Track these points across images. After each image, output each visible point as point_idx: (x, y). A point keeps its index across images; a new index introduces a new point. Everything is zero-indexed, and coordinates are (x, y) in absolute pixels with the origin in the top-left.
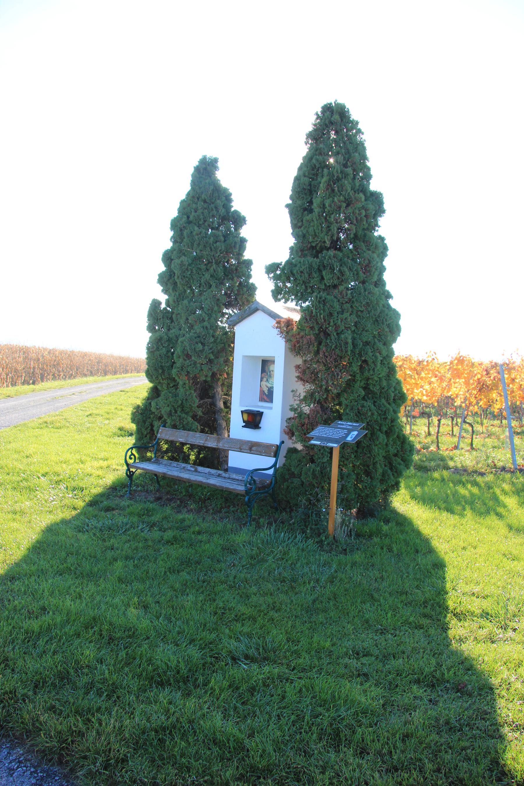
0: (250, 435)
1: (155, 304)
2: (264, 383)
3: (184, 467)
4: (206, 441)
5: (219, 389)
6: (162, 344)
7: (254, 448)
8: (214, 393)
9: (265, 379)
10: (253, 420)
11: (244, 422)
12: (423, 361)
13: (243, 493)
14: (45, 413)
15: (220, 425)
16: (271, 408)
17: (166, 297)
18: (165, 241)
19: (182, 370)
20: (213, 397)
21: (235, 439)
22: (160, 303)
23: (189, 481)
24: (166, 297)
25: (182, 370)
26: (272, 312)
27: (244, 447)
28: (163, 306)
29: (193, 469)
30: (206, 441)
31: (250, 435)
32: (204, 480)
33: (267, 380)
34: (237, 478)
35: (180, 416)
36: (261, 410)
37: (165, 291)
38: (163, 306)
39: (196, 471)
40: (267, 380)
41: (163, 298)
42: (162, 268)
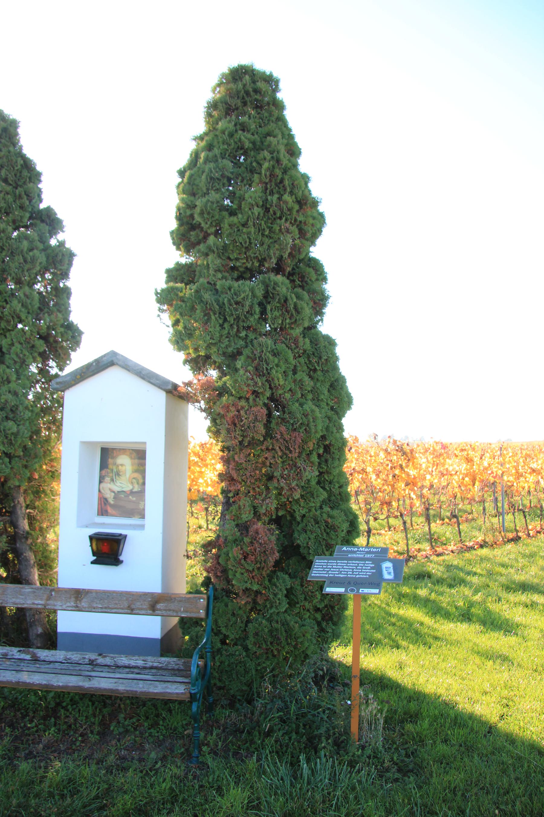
0: (104, 578)
2: (107, 485)
4: (49, 598)
5: (21, 499)
7: (159, 606)
8: (15, 506)
9: (108, 479)
10: (108, 549)
14: (127, 731)
15: (27, 560)
16: (142, 527)
18: (52, 195)
20: (12, 513)
21: (114, 592)
23: (47, 689)
26: (143, 369)
29: (28, 657)
30: (49, 598)
31: (104, 578)
32: (87, 684)
34: (133, 663)
36: (123, 532)
39: (36, 659)
40: (112, 480)
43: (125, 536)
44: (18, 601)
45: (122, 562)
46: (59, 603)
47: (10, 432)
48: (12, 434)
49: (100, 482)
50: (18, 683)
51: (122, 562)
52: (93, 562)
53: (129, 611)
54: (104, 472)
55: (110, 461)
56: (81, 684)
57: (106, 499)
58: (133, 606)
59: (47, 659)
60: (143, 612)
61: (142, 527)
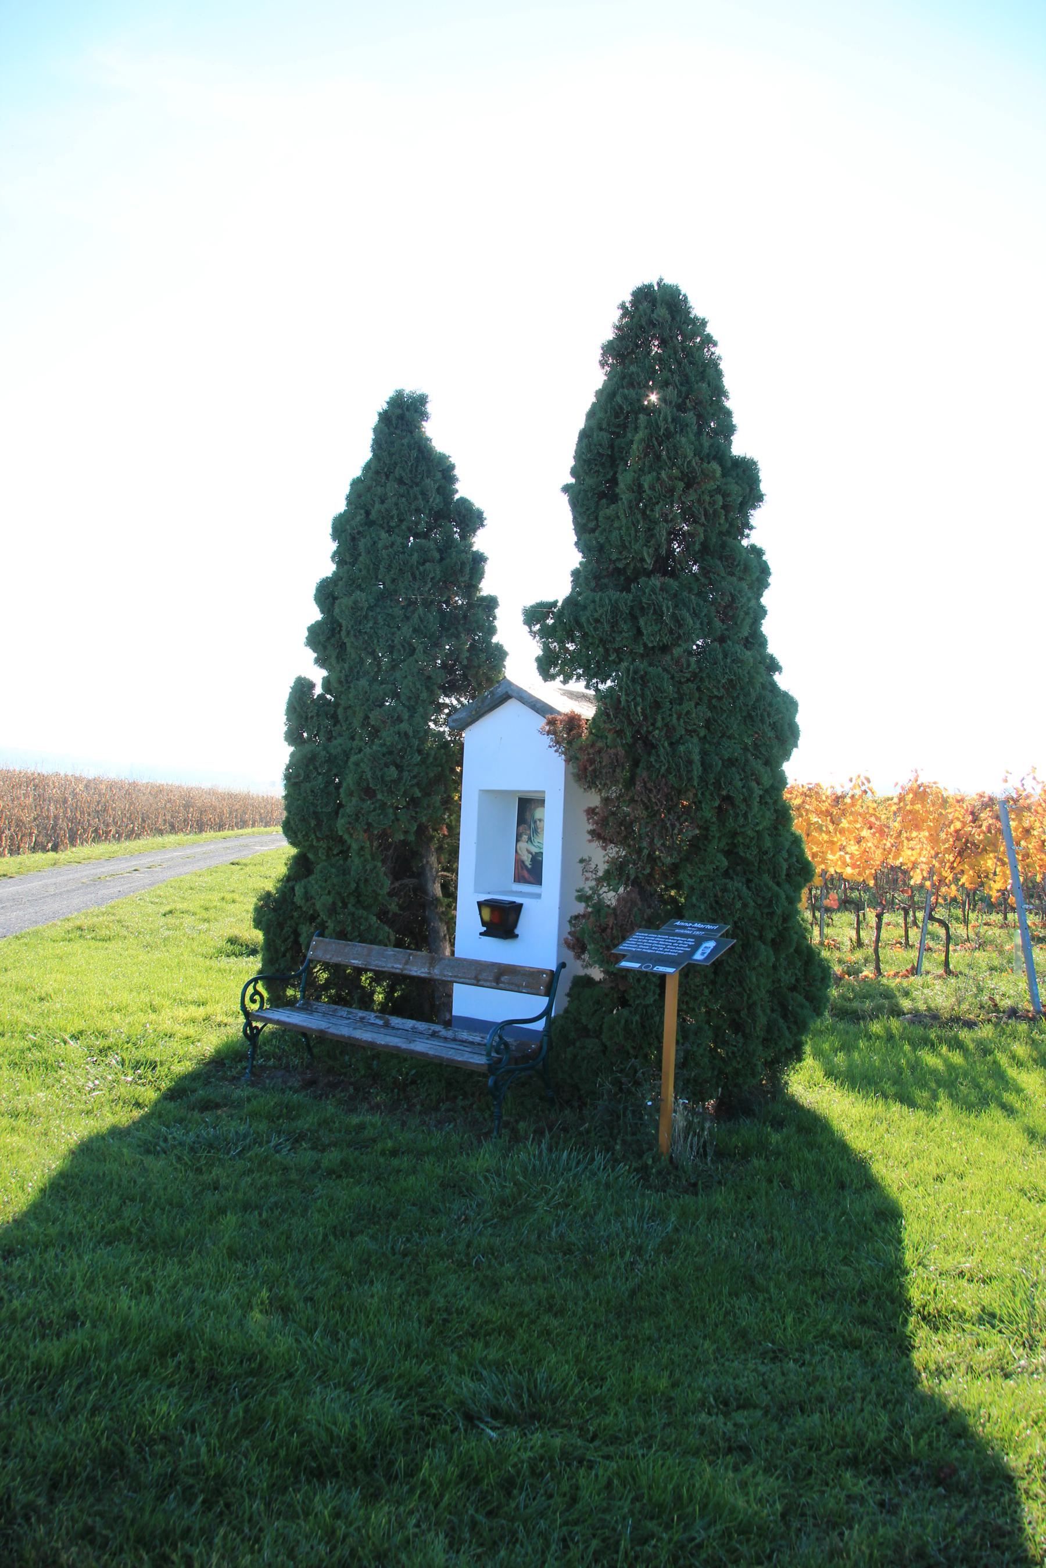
1: (302, 687)
2: (523, 845)
3: (362, 1018)
4: (407, 963)
5: (433, 859)
6: (316, 768)
7: (504, 978)
8: (423, 867)
9: (525, 837)
10: (502, 920)
11: (484, 924)
12: (843, 797)
13: (485, 1069)
14: (79, 910)
16: (538, 896)
17: (324, 673)
18: (321, 561)
19: (357, 819)
20: (420, 874)
21: (465, 960)
22: (312, 686)
23: (372, 1045)
24: (324, 673)
25: (357, 819)
26: (538, 701)
27: (484, 975)
28: (318, 690)
29: (381, 1023)
30: (407, 963)
32: (404, 1046)
33: (530, 839)
34: (471, 1038)
35: (353, 914)
37: (321, 662)
38: (318, 690)
39: (387, 1025)
40: (530, 839)
41: (318, 675)
42: (316, 615)
43: (521, 905)
44: (380, 963)
45: (517, 936)
46: (415, 969)
47: (388, 779)
48: (392, 781)
49: (517, 841)
50: (349, 1038)
51: (517, 936)
52: (481, 934)
53: (475, 982)
54: (521, 828)
55: (528, 816)
56: (399, 1045)
57: (523, 862)
58: (480, 977)
59: (397, 1026)
60: (488, 984)
61: (538, 896)
